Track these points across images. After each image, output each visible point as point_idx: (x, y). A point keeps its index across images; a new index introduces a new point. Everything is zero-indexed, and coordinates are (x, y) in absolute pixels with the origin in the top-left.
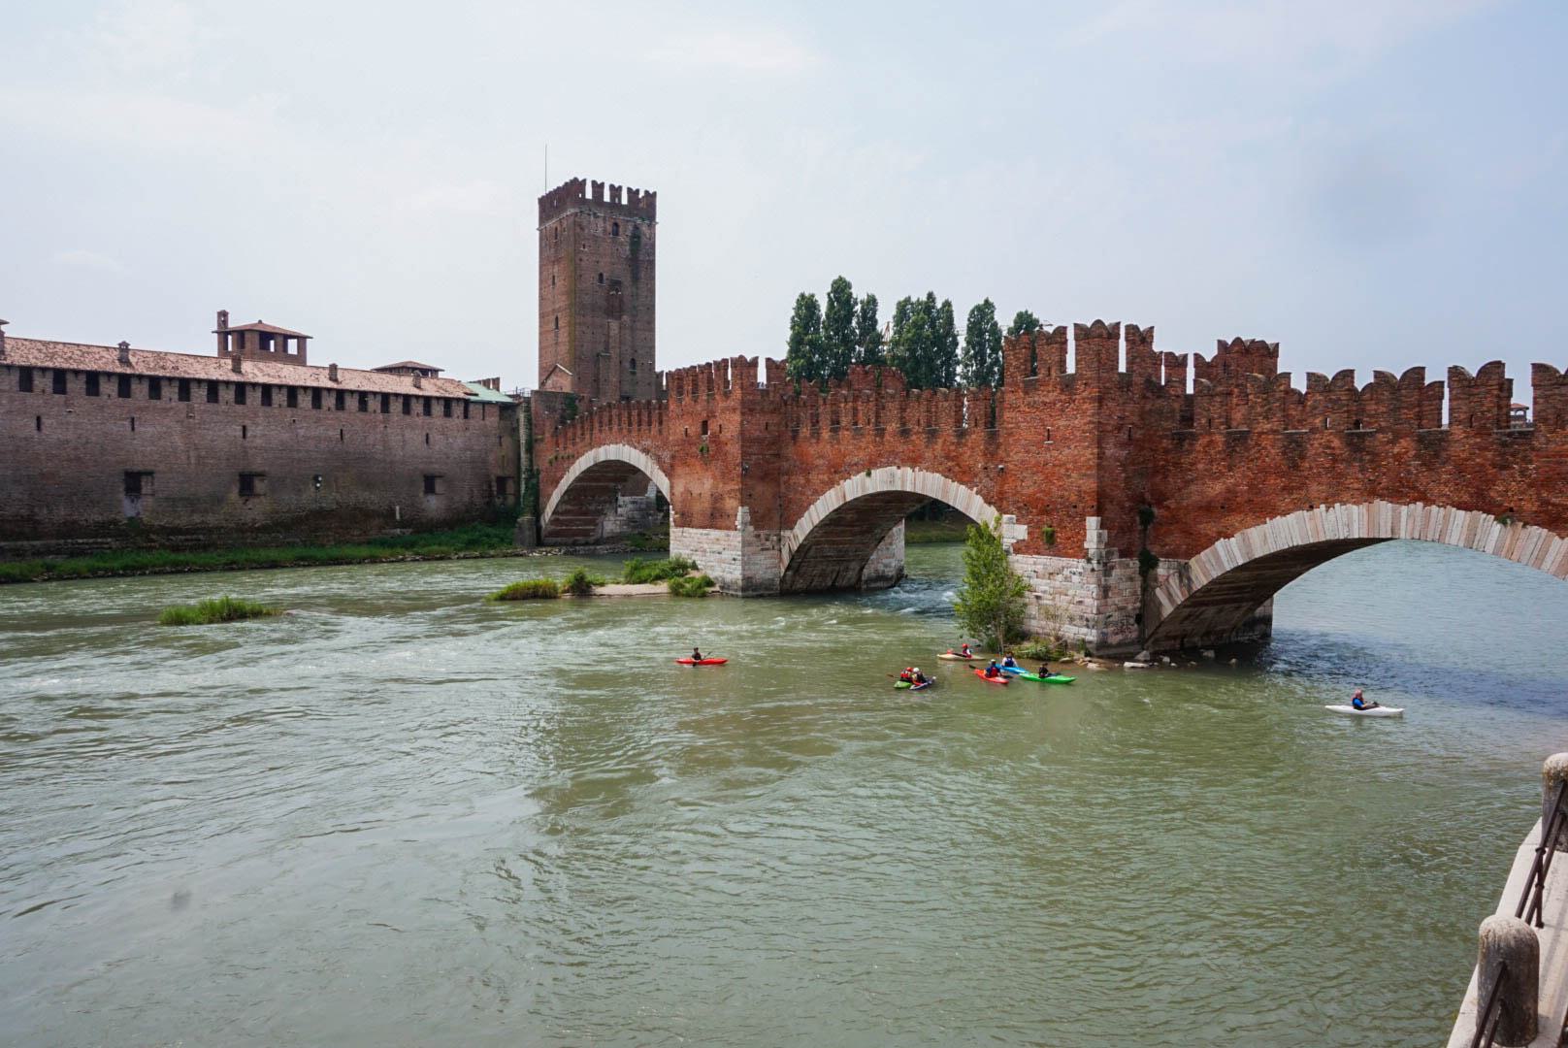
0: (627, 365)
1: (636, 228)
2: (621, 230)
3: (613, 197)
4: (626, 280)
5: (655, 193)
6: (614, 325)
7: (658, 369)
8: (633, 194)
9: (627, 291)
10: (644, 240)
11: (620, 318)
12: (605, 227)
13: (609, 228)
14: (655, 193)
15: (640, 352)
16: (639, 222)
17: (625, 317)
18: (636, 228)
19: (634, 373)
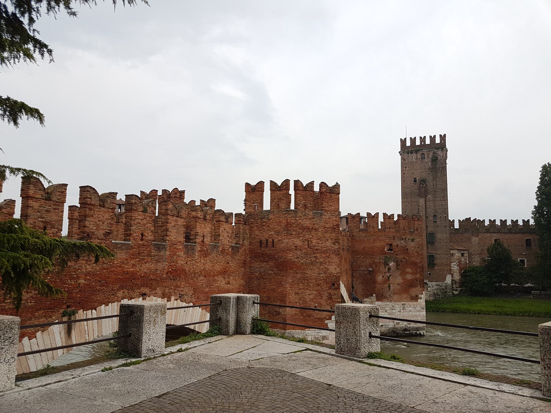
0: (431, 218)
1: (434, 153)
2: (426, 156)
3: (421, 142)
4: (430, 179)
5: (445, 135)
6: (422, 201)
7: (451, 218)
8: (433, 139)
9: (430, 184)
10: (439, 158)
11: (426, 197)
12: (417, 157)
13: (419, 156)
14: (445, 135)
15: (439, 211)
16: (435, 150)
17: (429, 196)
18: (434, 153)
19: (435, 222)
